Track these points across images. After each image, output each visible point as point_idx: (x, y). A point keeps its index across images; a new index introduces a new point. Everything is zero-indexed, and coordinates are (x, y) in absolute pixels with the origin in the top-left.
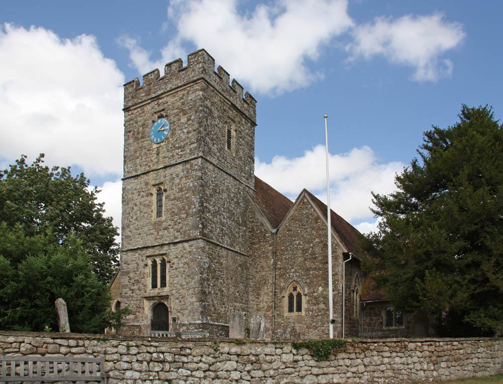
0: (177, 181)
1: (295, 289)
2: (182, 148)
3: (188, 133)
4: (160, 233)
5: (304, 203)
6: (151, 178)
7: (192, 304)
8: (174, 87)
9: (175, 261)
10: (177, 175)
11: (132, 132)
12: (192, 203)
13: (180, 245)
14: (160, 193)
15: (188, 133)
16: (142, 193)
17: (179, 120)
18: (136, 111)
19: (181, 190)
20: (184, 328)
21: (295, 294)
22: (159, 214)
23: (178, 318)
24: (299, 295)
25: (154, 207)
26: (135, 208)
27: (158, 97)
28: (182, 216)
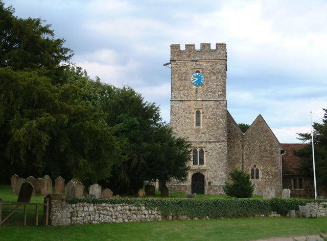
0: (211, 109)
1: (255, 166)
2: (214, 93)
3: (217, 85)
4: (200, 135)
5: (259, 121)
6: (192, 104)
7: (222, 175)
8: (207, 58)
9: (210, 151)
10: (211, 106)
11: (177, 75)
12: (220, 123)
13: (214, 144)
14: (198, 114)
15: (217, 85)
16: (186, 111)
17: (210, 77)
18: (179, 63)
19: (213, 114)
20: (217, 188)
21: (255, 169)
22: (198, 124)
23: (213, 183)
24: (257, 170)
25: (195, 120)
26: (181, 118)
27: (196, 61)
28: (214, 128)
